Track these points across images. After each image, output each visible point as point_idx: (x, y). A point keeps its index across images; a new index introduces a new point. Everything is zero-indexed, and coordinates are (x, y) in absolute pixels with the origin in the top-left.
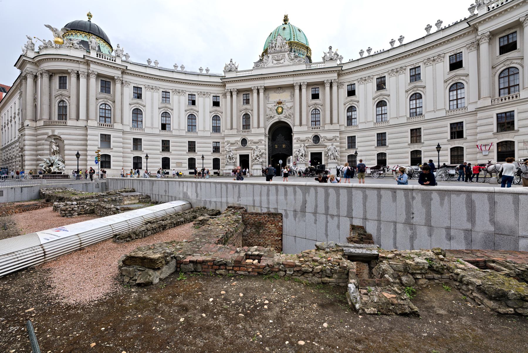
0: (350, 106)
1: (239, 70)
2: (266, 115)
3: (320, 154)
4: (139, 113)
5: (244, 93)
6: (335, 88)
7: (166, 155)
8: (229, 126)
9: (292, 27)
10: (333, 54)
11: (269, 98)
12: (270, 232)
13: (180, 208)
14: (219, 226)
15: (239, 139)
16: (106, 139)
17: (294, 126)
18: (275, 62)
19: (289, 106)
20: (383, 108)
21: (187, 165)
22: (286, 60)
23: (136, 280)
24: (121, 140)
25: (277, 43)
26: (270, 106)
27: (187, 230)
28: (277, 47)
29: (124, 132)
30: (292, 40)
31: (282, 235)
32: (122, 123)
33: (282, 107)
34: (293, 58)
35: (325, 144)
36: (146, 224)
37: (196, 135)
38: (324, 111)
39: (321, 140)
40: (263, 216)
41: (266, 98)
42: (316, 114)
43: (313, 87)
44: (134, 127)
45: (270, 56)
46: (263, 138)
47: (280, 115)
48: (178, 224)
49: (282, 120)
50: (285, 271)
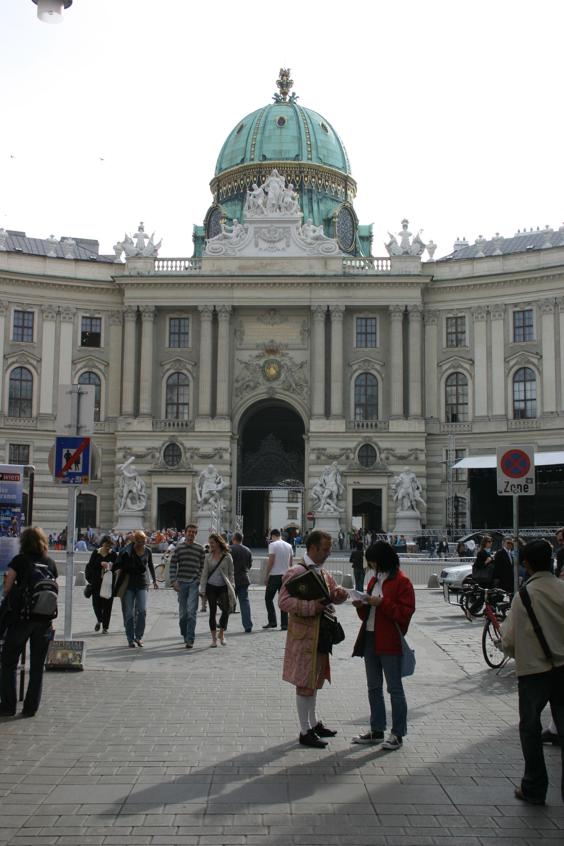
0: (452, 371)
1: (161, 254)
2: (232, 381)
3: (378, 492)
5: (174, 316)
6: (415, 327)
8: (128, 407)
9: (302, 117)
10: (411, 240)
11: (243, 333)
15: (158, 443)
17: (311, 417)
18: (263, 245)
19: (298, 362)
20: (528, 384)
22: (292, 243)
25: (270, 195)
26: (245, 356)
28: (269, 205)
30: (304, 161)
33: (278, 363)
34: (309, 241)
35: (392, 468)
38: (388, 380)
39: (381, 457)
41: (236, 333)
42: (366, 386)
43: (362, 315)
45: (251, 228)
46: (226, 444)
47: (275, 384)
49: (277, 396)
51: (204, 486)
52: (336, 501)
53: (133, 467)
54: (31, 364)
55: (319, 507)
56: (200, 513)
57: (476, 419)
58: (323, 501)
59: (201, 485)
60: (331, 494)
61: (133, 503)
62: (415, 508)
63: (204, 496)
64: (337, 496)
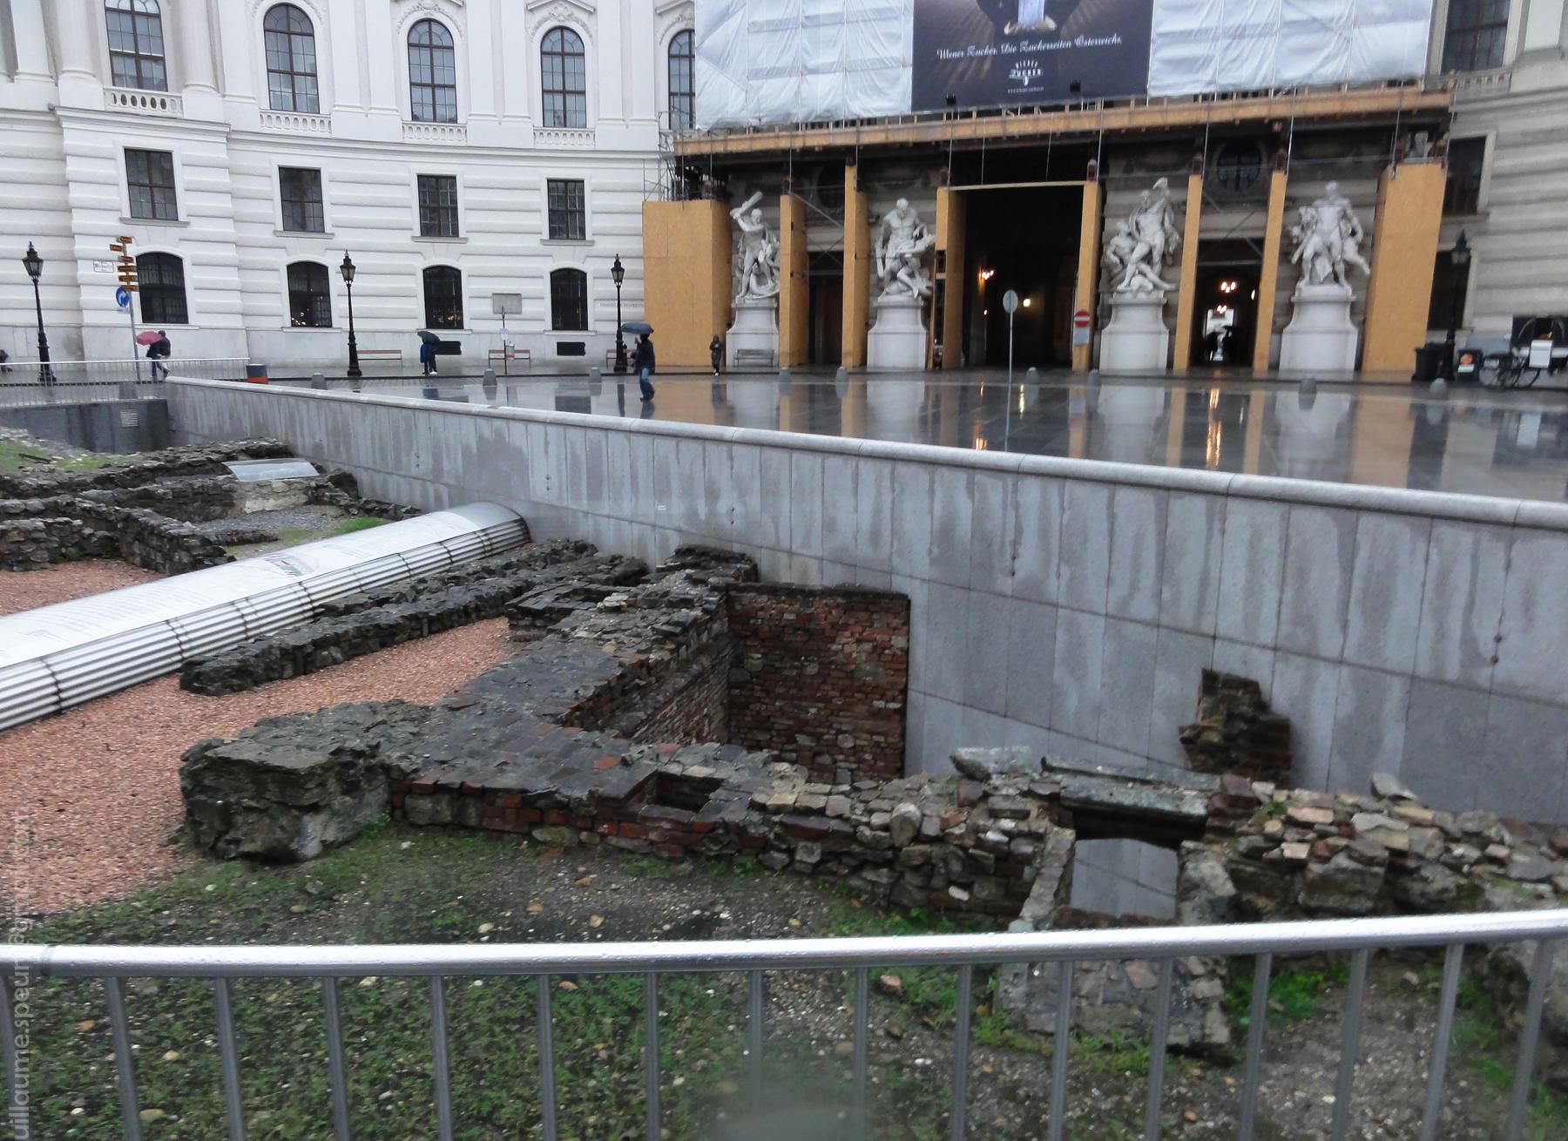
4: (295, 28)
7: (441, 253)
14: (597, 643)
16: (151, 175)
21: (544, 308)
23: (237, 842)
24: (223, 179)
27: (475, 651)
29: (232, 137)
31: (904, 691)
32: (218, 85)
36: (316, 617)
37: (583, 143)
44: (276, 105)
48: (441, 623)
50: (791, 852)
51: (891, 245)
52: (1158, 268)
53: (757, 213)
54: (577, 21)
55: (1122, 281)
56: (882, 299)
57: (1524, 57)
58: (1130, 269)
59: (886, 242)
60: (1150, 253)
61: (759, 283)
62: (1342, 278)
63: (890, 264)
64: (1164, 256)
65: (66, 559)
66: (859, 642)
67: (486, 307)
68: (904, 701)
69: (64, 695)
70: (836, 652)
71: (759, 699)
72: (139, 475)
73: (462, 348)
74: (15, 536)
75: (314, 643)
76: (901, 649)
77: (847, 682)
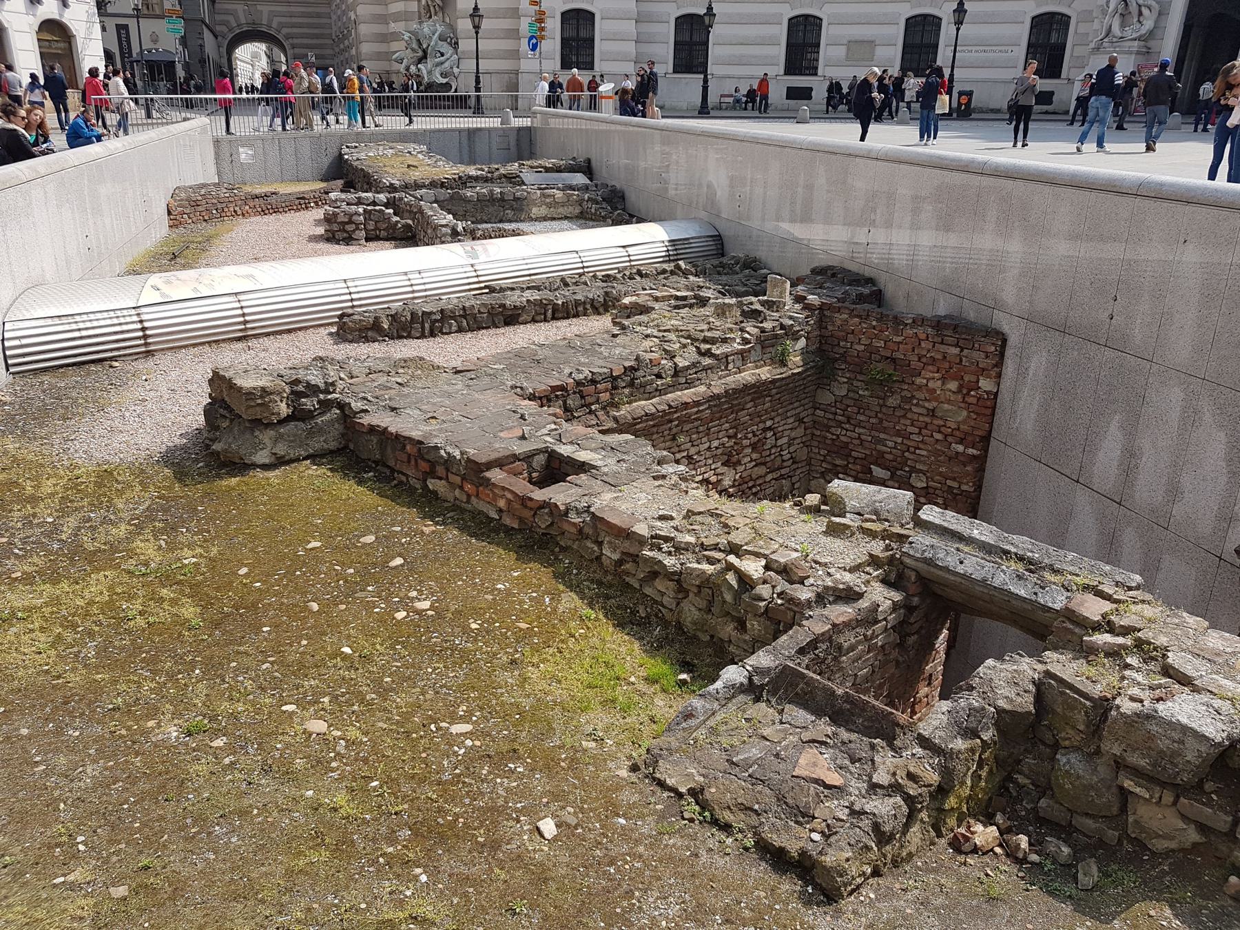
12: (932, 413)
13: (660, 250)
31: (986, 439)
40: (910, 332)
65: (377, 238)
66: (944, 379)
67: (841, 52)
68: (986, 450)
69: (249, 326)
70: (920, 387)
71: (839, 424)
72: (464, 181)
73: (813, 94)
74: (342, 218)
75: (442, 311)
76: (987, 393)
77: (928, 420)
